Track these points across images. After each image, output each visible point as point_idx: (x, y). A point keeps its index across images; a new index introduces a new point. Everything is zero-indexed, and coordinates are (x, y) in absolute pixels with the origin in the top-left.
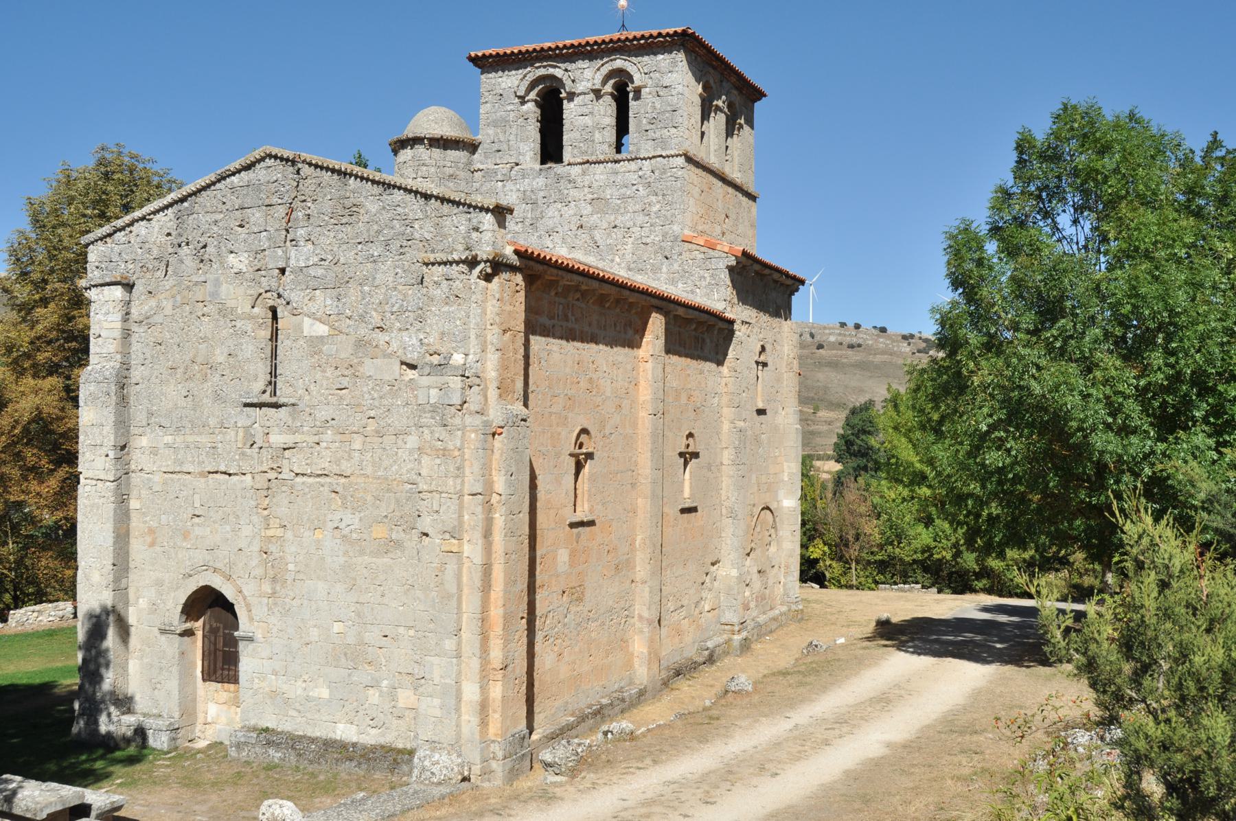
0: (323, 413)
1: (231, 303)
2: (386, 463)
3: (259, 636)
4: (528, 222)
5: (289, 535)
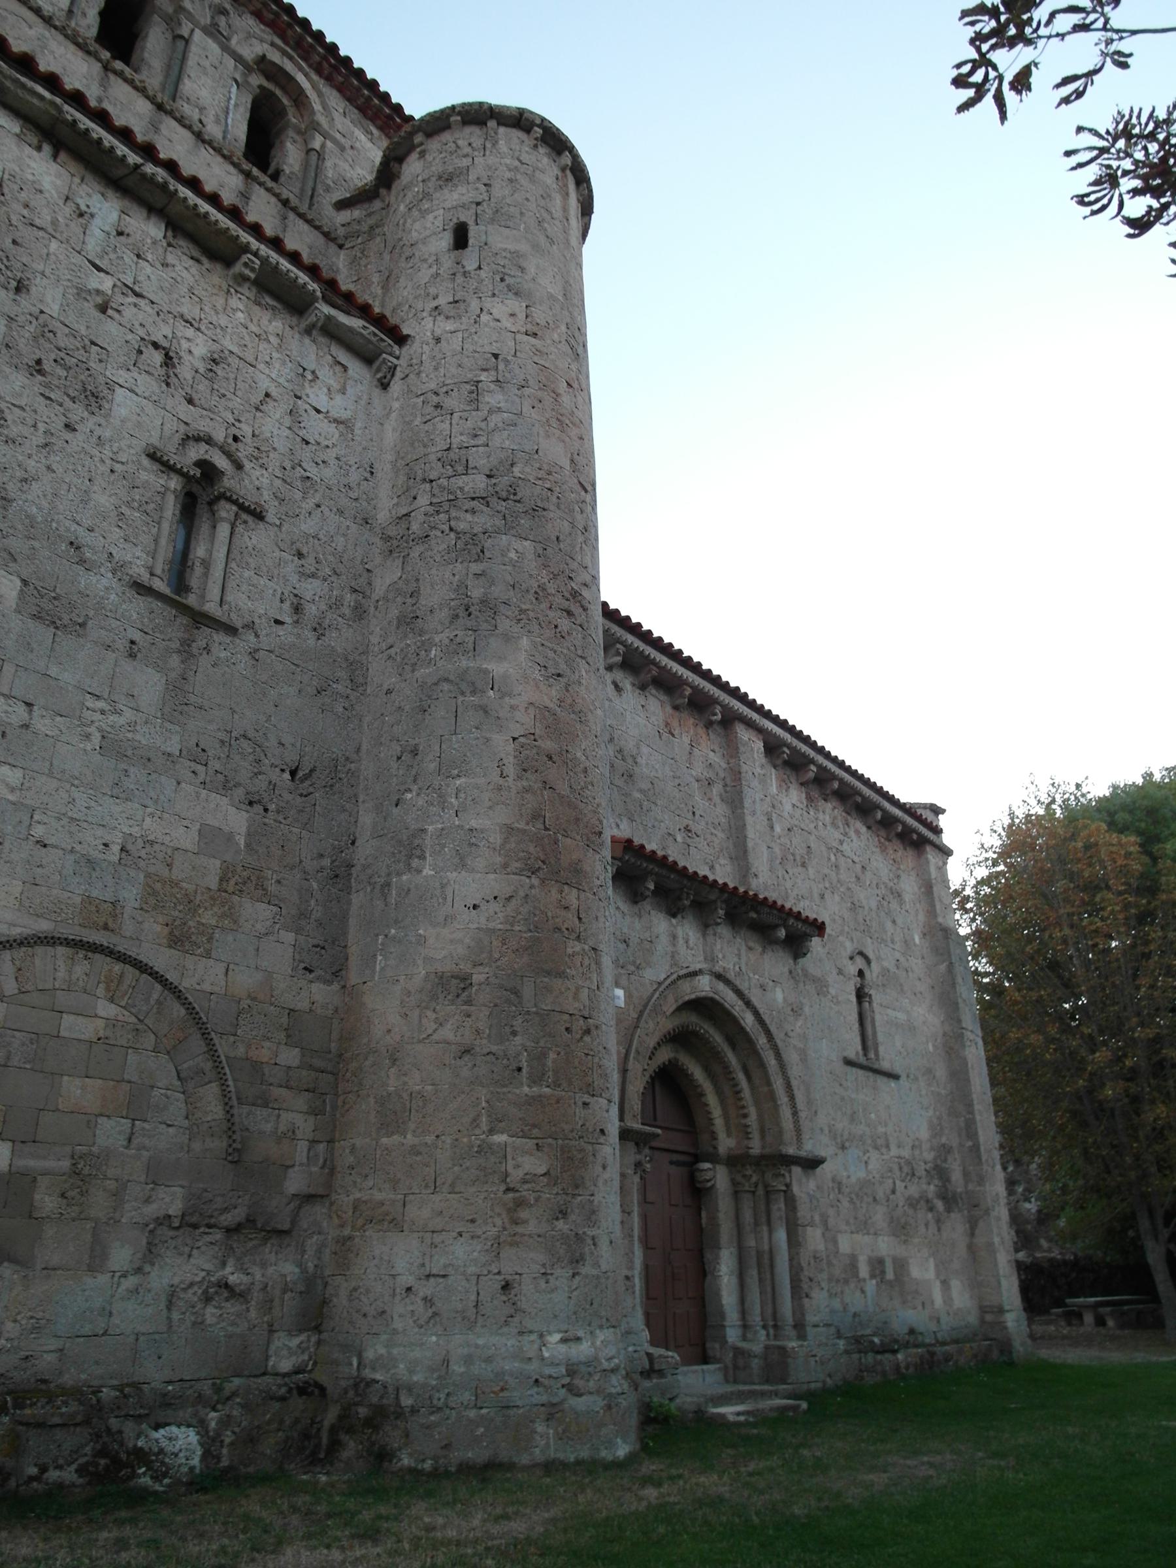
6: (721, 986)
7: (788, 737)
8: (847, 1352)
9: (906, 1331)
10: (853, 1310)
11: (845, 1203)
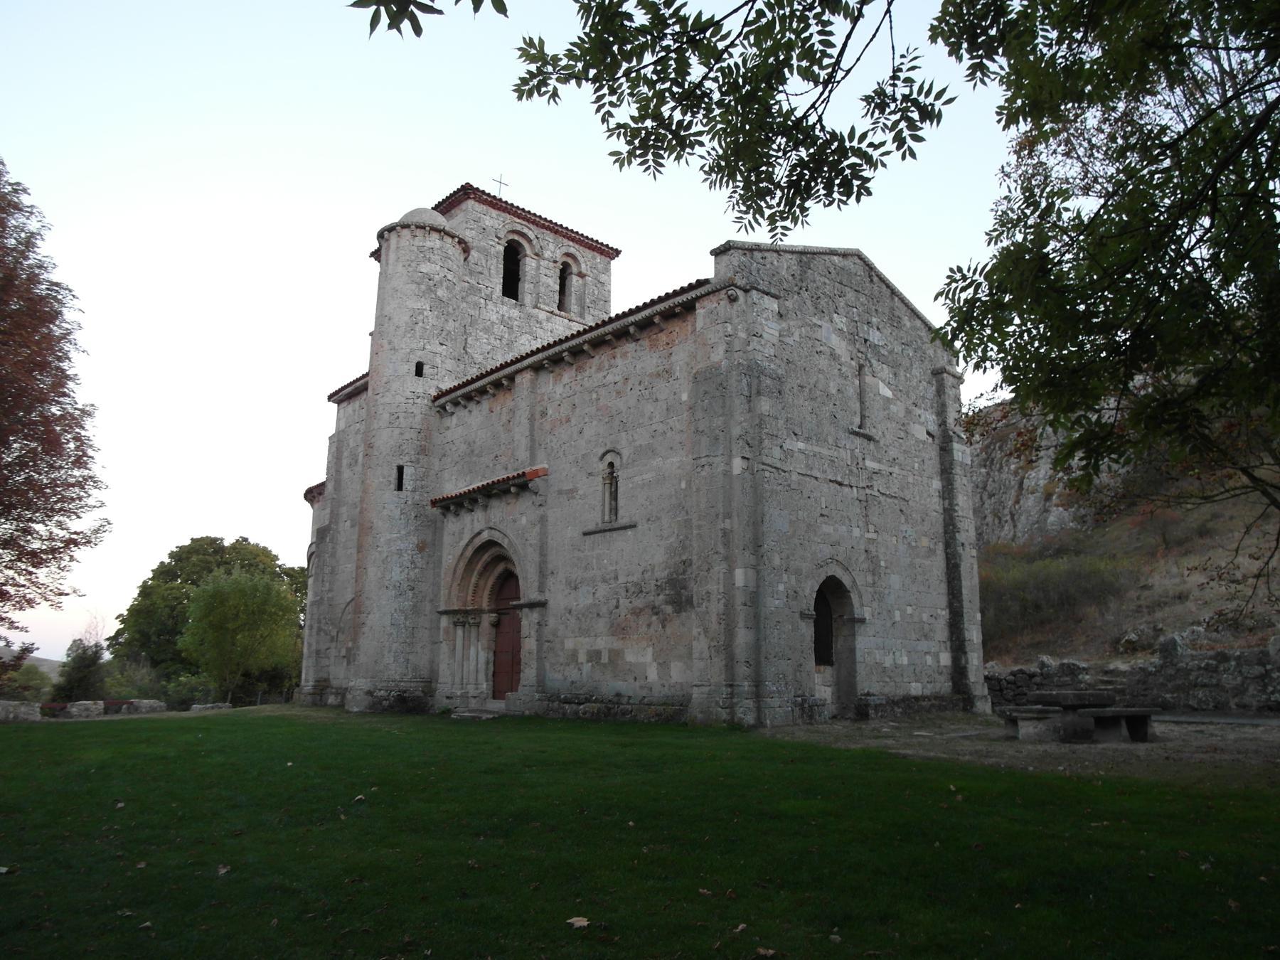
0: (893, 453)
1: (838, 351)
2: (925, 495)
3: (867, 616)
4: (504, 341)
5: (880, 539)
7: (540, 356)
9: (613, 693)
11: (573, 620)
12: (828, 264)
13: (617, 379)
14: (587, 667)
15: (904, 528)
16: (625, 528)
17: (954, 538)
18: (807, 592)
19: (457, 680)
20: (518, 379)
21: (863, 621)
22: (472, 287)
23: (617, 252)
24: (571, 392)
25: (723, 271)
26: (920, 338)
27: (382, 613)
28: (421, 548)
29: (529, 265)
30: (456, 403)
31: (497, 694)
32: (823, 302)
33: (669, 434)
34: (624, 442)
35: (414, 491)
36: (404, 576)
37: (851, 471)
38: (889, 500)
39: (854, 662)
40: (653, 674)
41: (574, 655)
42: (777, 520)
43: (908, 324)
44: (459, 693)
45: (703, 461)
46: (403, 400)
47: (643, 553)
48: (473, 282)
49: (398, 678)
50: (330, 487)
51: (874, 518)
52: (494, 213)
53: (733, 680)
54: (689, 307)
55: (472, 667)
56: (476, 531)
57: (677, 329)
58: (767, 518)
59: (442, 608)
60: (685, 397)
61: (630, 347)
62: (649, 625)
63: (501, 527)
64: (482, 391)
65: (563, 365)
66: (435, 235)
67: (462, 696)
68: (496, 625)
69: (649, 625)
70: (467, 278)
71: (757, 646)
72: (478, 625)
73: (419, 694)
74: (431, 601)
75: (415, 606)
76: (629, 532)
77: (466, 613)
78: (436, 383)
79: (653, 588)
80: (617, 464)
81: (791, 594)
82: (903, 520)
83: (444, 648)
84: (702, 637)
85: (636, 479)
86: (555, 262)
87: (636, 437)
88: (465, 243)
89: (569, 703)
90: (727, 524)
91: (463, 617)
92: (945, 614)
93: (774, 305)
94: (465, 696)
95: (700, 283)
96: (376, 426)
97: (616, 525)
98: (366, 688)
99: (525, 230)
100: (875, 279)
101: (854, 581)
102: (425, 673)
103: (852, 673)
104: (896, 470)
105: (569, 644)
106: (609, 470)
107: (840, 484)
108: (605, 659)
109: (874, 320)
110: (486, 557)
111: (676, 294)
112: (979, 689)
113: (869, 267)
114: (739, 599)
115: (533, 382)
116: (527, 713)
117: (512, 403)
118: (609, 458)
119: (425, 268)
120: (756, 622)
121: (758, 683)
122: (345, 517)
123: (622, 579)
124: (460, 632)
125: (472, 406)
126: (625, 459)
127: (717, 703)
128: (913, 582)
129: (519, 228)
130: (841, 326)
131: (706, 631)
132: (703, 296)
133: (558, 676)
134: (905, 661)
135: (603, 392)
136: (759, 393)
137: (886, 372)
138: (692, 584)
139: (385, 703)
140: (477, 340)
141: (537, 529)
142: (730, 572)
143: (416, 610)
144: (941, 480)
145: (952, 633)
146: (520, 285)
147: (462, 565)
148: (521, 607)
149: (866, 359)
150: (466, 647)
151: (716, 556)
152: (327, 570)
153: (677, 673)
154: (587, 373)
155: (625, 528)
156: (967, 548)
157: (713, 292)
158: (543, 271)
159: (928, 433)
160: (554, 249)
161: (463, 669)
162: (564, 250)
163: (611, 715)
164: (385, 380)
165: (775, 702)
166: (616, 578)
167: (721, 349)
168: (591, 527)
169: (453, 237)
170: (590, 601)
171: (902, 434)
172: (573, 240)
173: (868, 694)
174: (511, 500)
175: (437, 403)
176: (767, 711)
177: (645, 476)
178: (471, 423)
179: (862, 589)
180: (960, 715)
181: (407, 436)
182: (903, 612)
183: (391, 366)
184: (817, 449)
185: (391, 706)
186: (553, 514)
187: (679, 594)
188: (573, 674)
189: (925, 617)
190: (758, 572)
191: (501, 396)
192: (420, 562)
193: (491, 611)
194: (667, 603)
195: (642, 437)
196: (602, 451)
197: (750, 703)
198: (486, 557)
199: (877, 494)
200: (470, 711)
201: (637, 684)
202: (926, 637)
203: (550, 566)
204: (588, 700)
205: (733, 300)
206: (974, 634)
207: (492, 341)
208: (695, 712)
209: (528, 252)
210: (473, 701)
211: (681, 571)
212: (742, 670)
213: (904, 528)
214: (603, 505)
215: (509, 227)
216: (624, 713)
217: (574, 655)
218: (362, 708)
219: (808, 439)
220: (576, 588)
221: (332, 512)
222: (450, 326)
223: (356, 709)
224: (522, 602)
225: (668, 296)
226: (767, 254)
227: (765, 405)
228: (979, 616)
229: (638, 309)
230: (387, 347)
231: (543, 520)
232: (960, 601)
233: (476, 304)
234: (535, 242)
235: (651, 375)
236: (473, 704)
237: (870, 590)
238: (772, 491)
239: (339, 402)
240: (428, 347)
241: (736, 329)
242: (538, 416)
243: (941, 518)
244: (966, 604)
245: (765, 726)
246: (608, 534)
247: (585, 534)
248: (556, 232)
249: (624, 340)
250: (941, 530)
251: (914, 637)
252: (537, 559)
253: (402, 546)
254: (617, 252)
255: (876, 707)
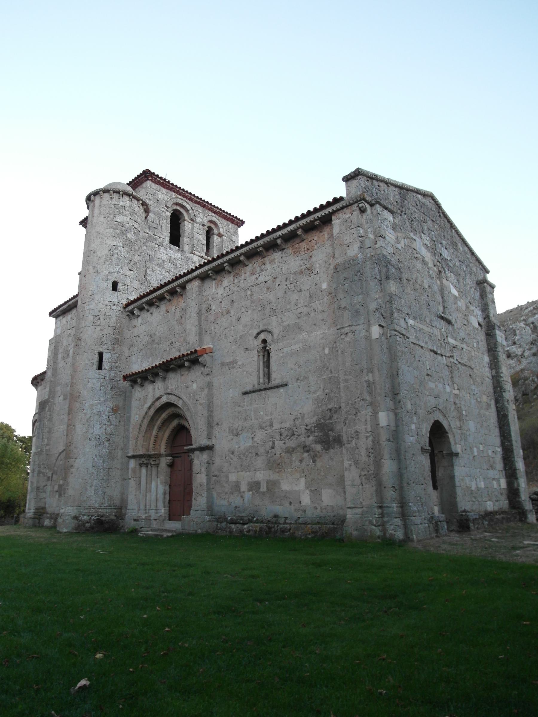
0: (462, 334)
1: (426, 259)
3: (459, 450)
5: (461, 395)
6: (170, 396)
7: (206, 268)
8: (210, 521)
9: (272, 515)
10: (234, 505)
11: (235, 459)
12: (416, 200)
13: (267, 279)
14: (248, 495)
15: (473, 387)
16: (278, 387)
17: (501, 396)
18: (424, 432)
19: (142, 507)
20: (189, 286)
21: (457, 455)
22: (150, 236)
23: (242, 223)
24: (230, 292)
25: (353, 192)
26: (468, 258)
27: (86, 458)
28: (115, 410)
29: (187, 226)
30: (141, 309)
31: (172, 516)
32: (415, 224)
33: (312, 314)
34: (274, 324)
35: (110, 370)
36: (103, 430)
37: (441, 344)
38: (463, 367)
39: (454, 486)
40: (306, 499)
41: (237, 486)
42: (408, 375)
43: (461, 248)
44: (144, 517)
45: (347, 330)
46: (103, 307)
47: (296, 405)
48: (151, 233)
49: (97, 505)
50: (49, 374)
51: (456, 380)
52: (164, 191)
53: (382, 502)
54: (327, 221)
55: (153, 497)
56: (157, 396)
57: (315, 238)
58: (400, 372)
59: (131, 454)
60: (324, 286)
61: (277, 255)
62: (301, 461)
63: (176, 392)
64: (161, 298)
65: (223, 273)
66: (126, 198)
67: (146, 518)
68: (171, 465)
69: (301, 461)
70: (147, 230)
71: (400, 474)
72: (157, 466)
73: (113, 517)
74: (122, 449)
75: (110, 453)
76: (281, 390)
77: (149, 456)
78: (126, 296)
79: (304, 431)
80: (269, 339)
81: (416, 434)
82: (472, 383)
83: (132, 482)
84: (353, 467)
85: (286, 350)
86: (204, 225)
87: (284, 319)
88: (147, 205)
89: (235, 523)
90: (370, 377)
91: (146, 460)
92: (499, 450)
93: (390, 217)
94: (148, 519)
95: (336, 200)
96: (84, 325)
97: (270, 386)
98: (73, 514)
99: (185, 204)
100: (442, 215)
101: (450, 425)
102: (117, 502)
103: (453, 494)
104: (464, 346)
105: (233, 478)
106: (262, 345)
107: (436, 353)
108: (263, 488)
109: (443, 242)
110: (164, 415)
111: (316, 210)
112: (528, 506)
113: (438, 205)
114: (384, 436)
115: (199, 287)
116: (199, 531)
117: (184, 304)
118: (262, 336)
119: (119, 219)
120: (398, 454)
121: (403, 504)
122: (59, 393)
123: (276, 426)
124: (144, 470)
125: (153, 309)
126: (275, 337)
127: (371, 522)
128: (481, 427)
129: (180, 201)
130: (426, 242)
131: (357, 463)
132: (338, 210)
133: (225, 503)
134: (482, 485)
135: (256, 289)
136: (387, 278)
137: (452, 277)
138: (338, 427)
139: (88, 525)
140: (153, 271)
141: (206, 391)
142: (375, 415)
143: (111, 455)
144: (489, 356)
145: (505, 465)
146: (181, 239)
147: (146, 422)
148: (193, 450)
149: (442, 267)
150: (148, 483)
151: (363, 402)
152: (46, 430)
153: (329, 498)
154: (243, 277)
155: (278, 387)
156: (511, 403)
157: (347, 206)
158: (196, 230)
159: (479, 324)
160: (203, 217)
161: (146, 499)
162: (209, 218)
163: (271, 534)
164: (90, 293)
165: (417, 520)
166: (271, 425)
167: (356, 247)
168: (249, 388)
169: (138, 200)
170: (250, 443)
171: (466, 323)
172: (215, 212)
173: (465, 511)
174: (184, 372)
175: (127, 309)
176: (412, 527)
177: (293, 347)
178: (154, 320)
179: (454, 430)
180: (520, 524)
181: (106, 331)
182: (478, 448)
183: (95, 283)
184: (421, 326)
185: (92, 528)
186: (217, 381)
187: (327, 435)
188: (236, 500)
189: (490, 452)
190: (396, 415)
191: (175, 300)
192: (114, 421)
193: (167, 455)
194: (316, 442)
195: (290, 319)
196: (256, 332)
197: (398, 521)
198: (164, 415)
199: (456, 362)
200: (152, 530)
201: (292, 507)
202: (492, 467)
203: (216, 419)
204: (250, 521)
205: (363, 211)
206: (520, 465)
207: (163, 272)
208: (350, 531)
209: (186, 218)
210: (154, 523)
211: (328, 417)
212: (390, 494)
213: (473, 387)
214: (259, 371)
215: (174, 201)
216: (283, 531)
217: (237, 486)
218: (69, 529)
219: (415, 318)
220: (237, 435)
221: (50, 390)
222: (136, 258)
223: (65, 530)
224: (194, 446)
225: (309, 213)
226: (381, 184)
227: (393, 287)
228: (521, 451)
229: (285, 225)
230: (92, 271)
231: (210, 385)
232: (510, 441)
233: (153, 248)
234: (191, 211)
235: (295, 273)
236: (155, 525)
237: (459, 431)
238: (402, 352)
239: (56, 317)
240: (121, 271)
241: (366, 232)
242: (204, 311)
243: (491, 382)
244: (514, 443)
245: (412, 541)
246: (263, 392)
247: (244, 394)
248: (204, 206)
249: (272, 251)
250: (492, 391)
251: (485, 467)
252: (206, 414)
253: (101, 409)
254: (242, 223)
255: (474, 520)
